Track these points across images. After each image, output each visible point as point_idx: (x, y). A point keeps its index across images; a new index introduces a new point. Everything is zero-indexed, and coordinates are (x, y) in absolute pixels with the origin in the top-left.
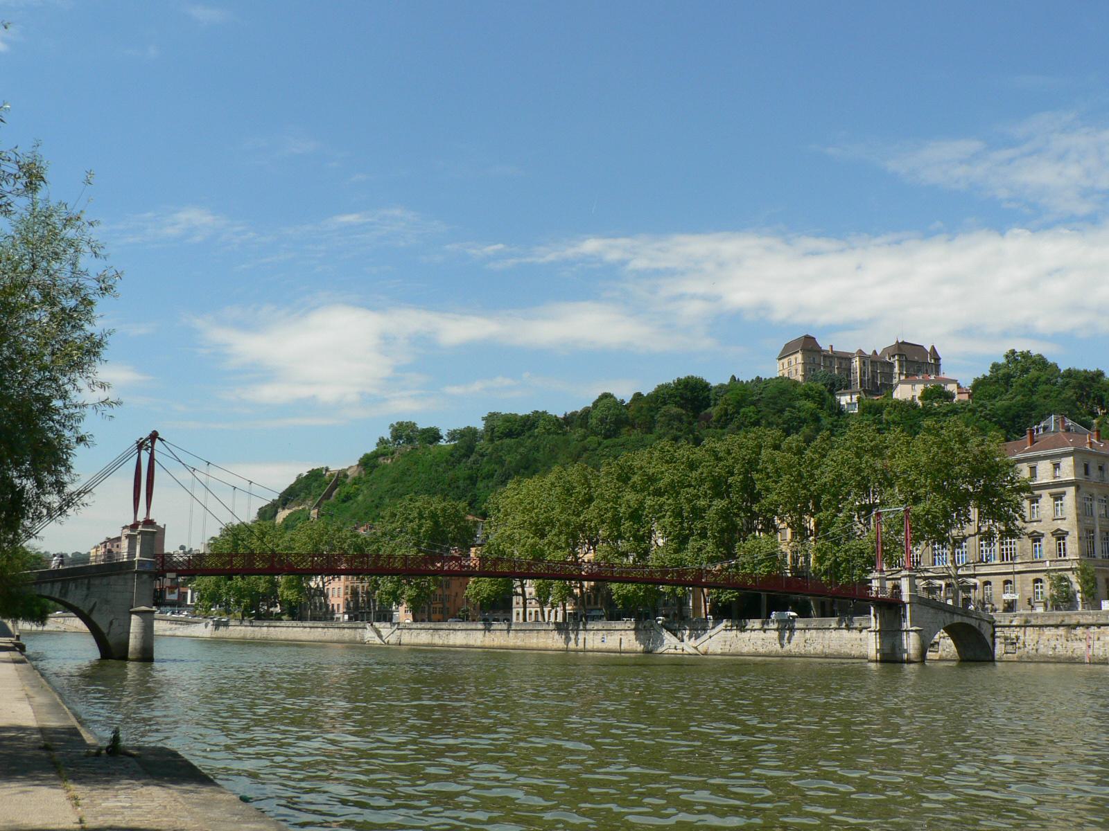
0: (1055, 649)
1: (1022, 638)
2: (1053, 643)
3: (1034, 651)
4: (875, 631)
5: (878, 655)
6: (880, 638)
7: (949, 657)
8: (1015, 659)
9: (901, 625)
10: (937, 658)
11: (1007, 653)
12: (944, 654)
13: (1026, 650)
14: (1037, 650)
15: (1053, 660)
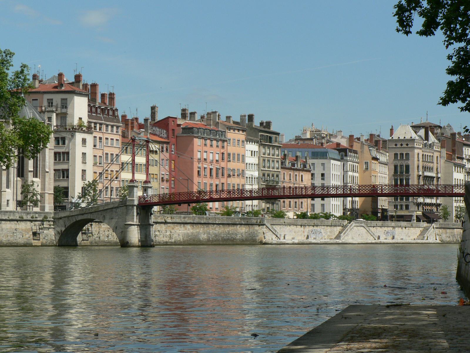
0: (108, 237)
1: (90, 229)
2: (107, 233)
3: (98, 238)
4: (138, 225)
5: (140, 243)
6: (140, 230)
7: (48, 244)
8: (89, 244)
9: (148, 221)
10: (40, 244)
11: (83, 240)
12: (44, 241)
13: (94, 237)
14: (99, 237)
15: (108, 244)
